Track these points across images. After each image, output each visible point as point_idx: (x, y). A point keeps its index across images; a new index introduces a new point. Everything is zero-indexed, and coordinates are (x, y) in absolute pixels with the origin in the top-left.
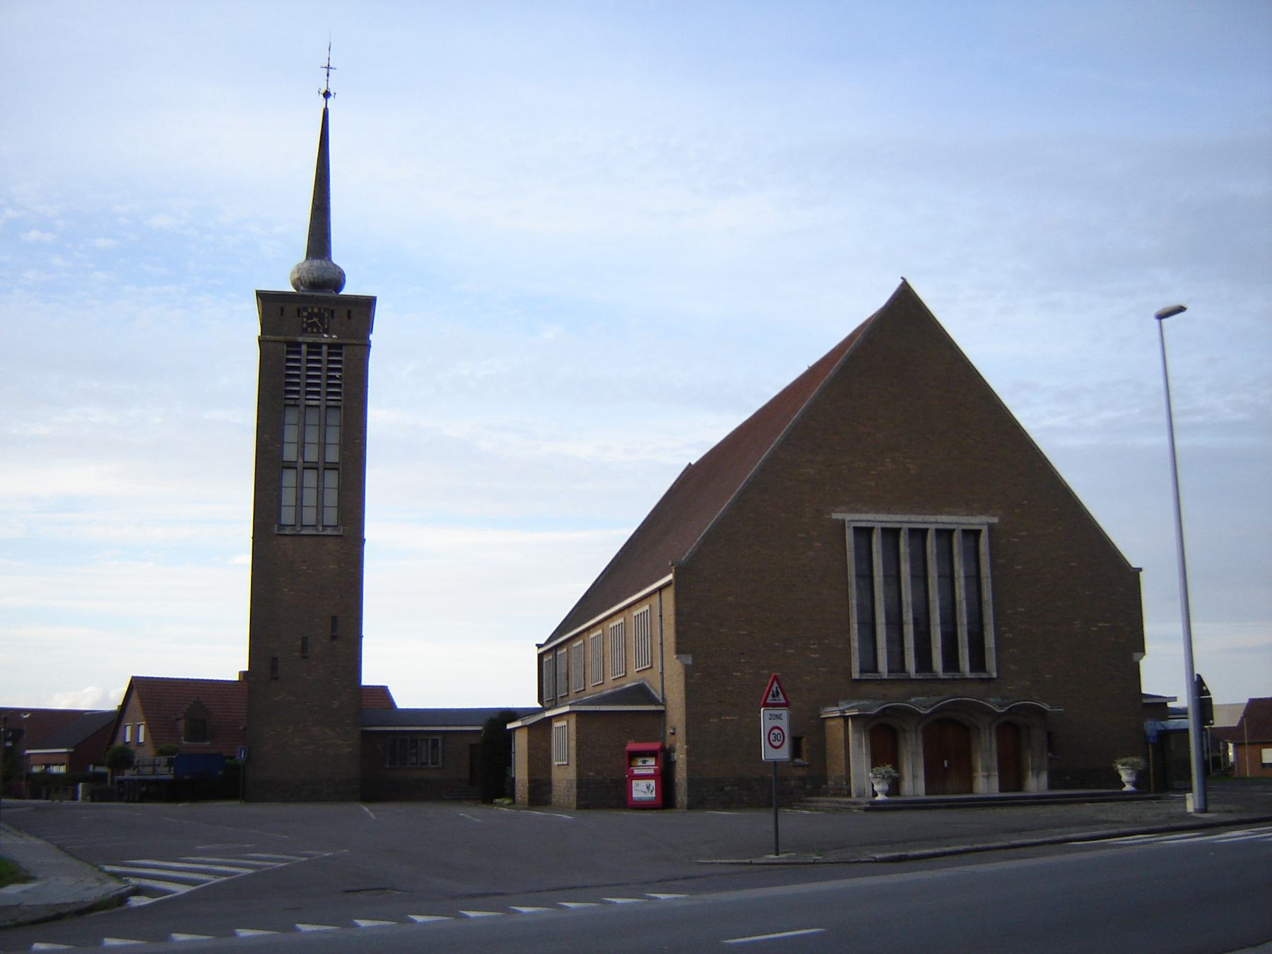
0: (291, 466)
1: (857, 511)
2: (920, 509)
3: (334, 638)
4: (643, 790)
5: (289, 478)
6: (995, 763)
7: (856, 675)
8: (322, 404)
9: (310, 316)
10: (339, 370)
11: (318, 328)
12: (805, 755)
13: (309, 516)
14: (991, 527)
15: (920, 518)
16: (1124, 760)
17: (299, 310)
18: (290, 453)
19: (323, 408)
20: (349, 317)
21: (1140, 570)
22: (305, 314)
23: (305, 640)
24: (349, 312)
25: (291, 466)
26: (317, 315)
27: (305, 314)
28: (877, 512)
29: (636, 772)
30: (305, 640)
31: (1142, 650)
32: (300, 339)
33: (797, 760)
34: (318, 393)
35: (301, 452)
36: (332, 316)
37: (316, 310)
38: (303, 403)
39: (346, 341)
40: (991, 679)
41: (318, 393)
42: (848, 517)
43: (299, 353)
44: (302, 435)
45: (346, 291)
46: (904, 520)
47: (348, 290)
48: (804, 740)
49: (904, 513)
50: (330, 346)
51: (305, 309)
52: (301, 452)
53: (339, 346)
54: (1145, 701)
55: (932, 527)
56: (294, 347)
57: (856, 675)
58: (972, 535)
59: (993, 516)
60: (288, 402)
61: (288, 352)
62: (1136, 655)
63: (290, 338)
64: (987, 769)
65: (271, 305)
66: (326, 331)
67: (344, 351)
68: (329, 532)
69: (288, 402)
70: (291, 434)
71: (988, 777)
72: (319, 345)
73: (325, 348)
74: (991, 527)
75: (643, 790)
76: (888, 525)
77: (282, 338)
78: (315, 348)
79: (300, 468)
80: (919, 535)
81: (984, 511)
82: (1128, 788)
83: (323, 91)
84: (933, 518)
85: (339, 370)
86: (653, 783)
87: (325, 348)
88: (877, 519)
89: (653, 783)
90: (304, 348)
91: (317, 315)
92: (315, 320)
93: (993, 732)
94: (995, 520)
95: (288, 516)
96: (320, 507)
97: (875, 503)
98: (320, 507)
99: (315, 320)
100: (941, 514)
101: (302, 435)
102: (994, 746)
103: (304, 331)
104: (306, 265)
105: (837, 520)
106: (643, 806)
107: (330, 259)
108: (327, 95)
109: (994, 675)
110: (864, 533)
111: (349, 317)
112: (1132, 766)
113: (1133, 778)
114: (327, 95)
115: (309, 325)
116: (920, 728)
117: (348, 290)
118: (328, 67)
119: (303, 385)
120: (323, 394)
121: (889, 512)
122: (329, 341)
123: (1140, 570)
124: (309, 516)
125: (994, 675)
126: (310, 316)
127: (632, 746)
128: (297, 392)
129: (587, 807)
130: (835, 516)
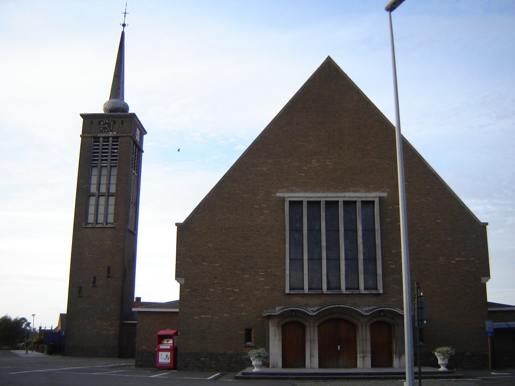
0: (93, 195)
1: (293, 191)
2: (335, 189)
3: (108, 277)
4: (164, 358)
5: (92, 201)
6: (369, 349)
7: (287, 291)
8: (108, 165)
9: (104, 124)
10: (117, 149)
11: (108, 130)
12: (253, 339)
13: (101, 219)
14: (381, 199)
15: (334, 195)
16: (440, 349)
17: (99, 122)
18: (93, 189)
19: (109, 167)
20: (122, 124)
21: (487, 224)
22: (102, 123)
23: (95, 278)
24: (122, 122)
25: (93, 195)
26: (107, 124)
27: (102, 123)
28: (306, 191)
29: (162, 347)
30: (95, 278)
31: (487, 275)
32: (99, 135)
33: (248, 343)
34: (107, 160)
35: (99, 189)
36: (115, 124)
37: (107, 121)
38: (99, 165)
39: (120, 135)
40: (379, 294)
41: (107, 160)
42: (286, 195)
43: (99, 142)
44: (109, 180)
45: (130, 112)
46: (323, 196)
47: (130, 111)
48: (253, 331)
49: (324, 192)
50: (114, 137)
51: (102, 121)
52: (99, 189)
53: (117, 137)
54: (490, 309)
55: (341, 200)
56: (97, 139)
57: (287, 291)
58: (368, 204)
59: (383, 192)
60: (93, 165)
61: (95, 142)
62: (483, 279)
63: (95, 135)
64: (364, 352)
65: (89, 120)
66: (111, 131)
67: (120, 140)
68: (109, 226)
69: (93, 165)
70: (94, 180)
71: (363, 357)
72: (108, 138)
73: (111, 139)
74: (381, 199)
75: (164, 358)
76: (312, 199)
77: (91, 135)
78: (106, 139)
79: (97, 196)
80: (332, 205)
81: (376, 190)
82: (442, 369)
84: (342, 195)
85: (117, 149)
86: (169, 354)
87: (111, 139)
88: (304, 196)
89: (169, 354)
90: (101, 139)
91: (107, 124)
92: (106, 126)
93: (368, 328)
94: (385, 195)
95: (91, 219)
96: (106, 215)
97: (304, 187)
98: (106, 215)
99: (106, 126)
100: (349, 191)
101: (109, 180)
102: (369, 337)
103: (101, 132)
104: (109, 101)
105: (280, 197)
106: (164, 368)
107: (123, 99)
108: (124, 25)
109: (381, 291)
110: (296, 205)
111: (122, 124)
112: (443, 354)
113: (446, 362)
114: (124, 25)
115: (103, 128)
116: (316, 325)
117: (130, 111)
118: (125, 13)
119: (100, 157)
120: (109, 160)
121: (313, 191)
122: (112, 135)
123: (487, 224)
124: (101, 219)
125: (381, 291)
126: (104, 124)
127: (162, 332)
128: (97, 160)
129: (141, 366)
130: (278, 195)
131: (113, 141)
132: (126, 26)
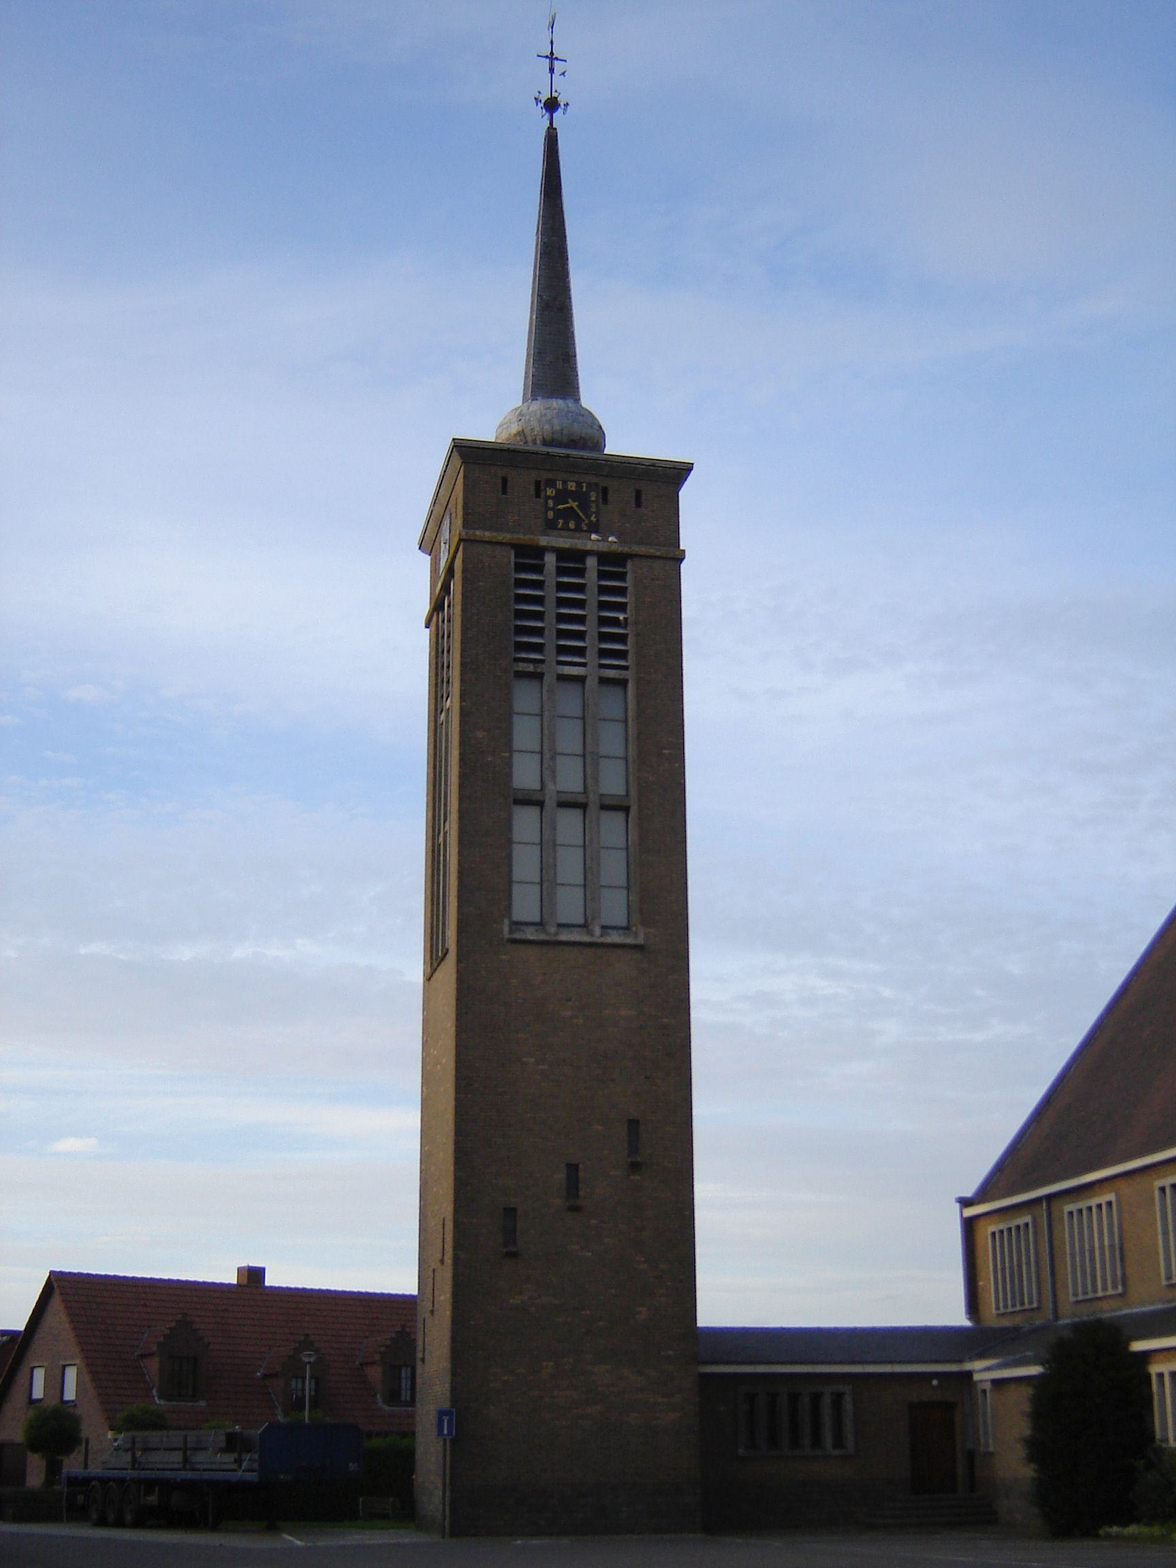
3: (635, 1167)
9: (562, 496)
11: (579, 520)
13: (570, 906)
17: (538, 484)
18: (525, 774)
20: (638, 504)
23: (573, 1169)
24: (638, 494)
26: (575, 495)
27: (550, 492)
30: (573, 1169)
32: (544, 541)
35: (548, 769)
36: (605, 500)
37: (572, 486)
38: (551, 670)
39: (636, 549)
43: (539, 569)
50: (604, 558)
51: (551, 483)
52: (548, 769)
53: (619, 559)
56: (529, 556)
60: (521, 667)
61: (519, 568)
66: (594, 528)
67: (629, 565)
69: (521, 667)
70: (525, 733)
72: (581, 555)
73: (591, 562)
77: (505, 537)
78: (571, 560)
83: (545, 96)
87: (591, 562)
90: (550, 560)
91: (575, 495)
92: (575, 505)
95: (525, 905)
96: (590, 884)
99: (575, 505)
103: (550, 526)
107: (577, 400)
108: (551, 105)
111: (638, 504)
114: (551, 105)
115: (559, 514)
122: (603, 547)
124: (570, 906)
126: (562, 496)
128: (539, 648)
131: (561, 571)
132: (560, 111)
